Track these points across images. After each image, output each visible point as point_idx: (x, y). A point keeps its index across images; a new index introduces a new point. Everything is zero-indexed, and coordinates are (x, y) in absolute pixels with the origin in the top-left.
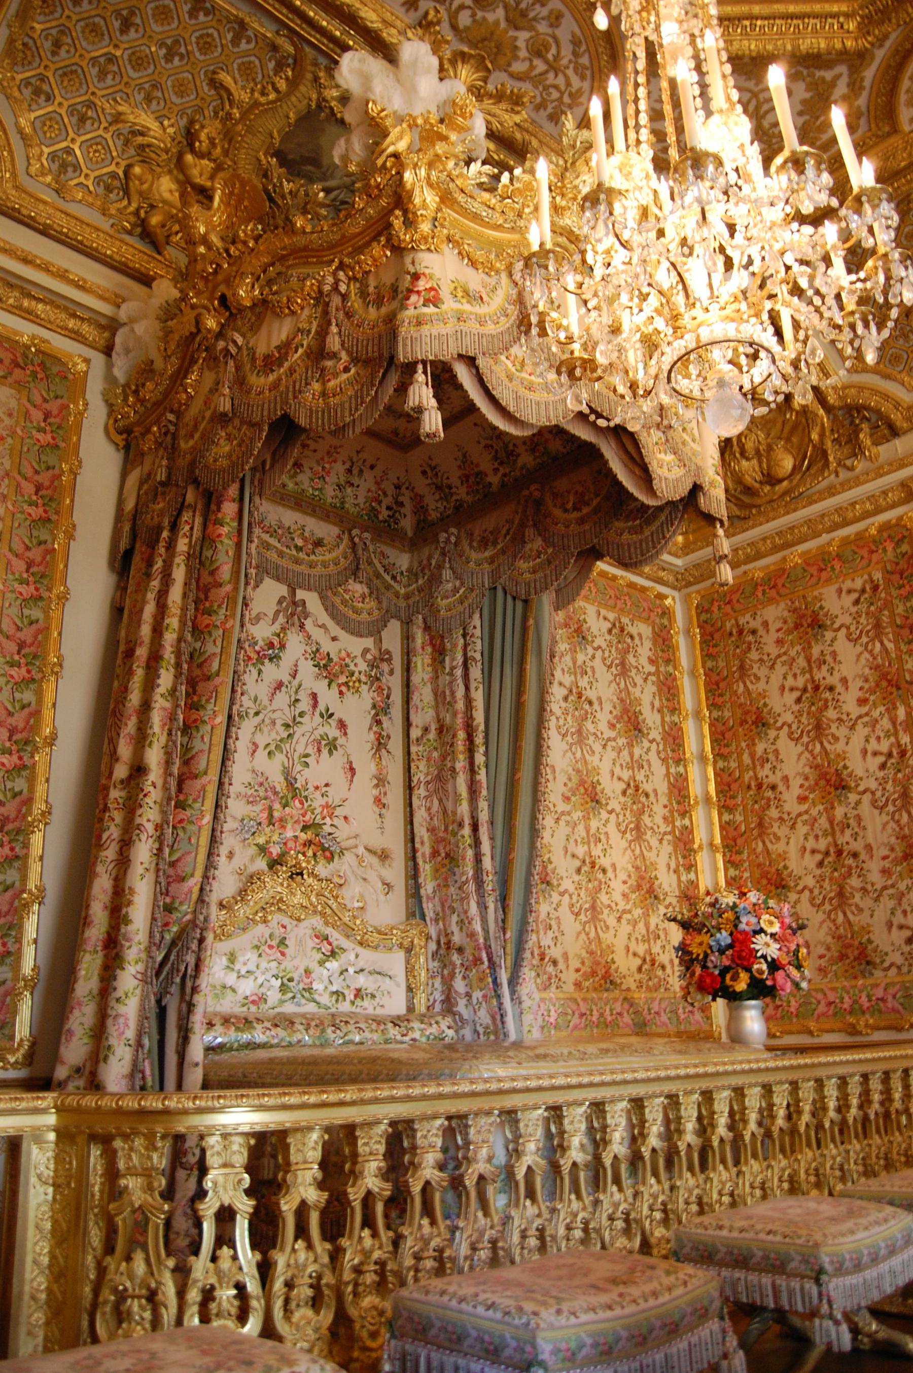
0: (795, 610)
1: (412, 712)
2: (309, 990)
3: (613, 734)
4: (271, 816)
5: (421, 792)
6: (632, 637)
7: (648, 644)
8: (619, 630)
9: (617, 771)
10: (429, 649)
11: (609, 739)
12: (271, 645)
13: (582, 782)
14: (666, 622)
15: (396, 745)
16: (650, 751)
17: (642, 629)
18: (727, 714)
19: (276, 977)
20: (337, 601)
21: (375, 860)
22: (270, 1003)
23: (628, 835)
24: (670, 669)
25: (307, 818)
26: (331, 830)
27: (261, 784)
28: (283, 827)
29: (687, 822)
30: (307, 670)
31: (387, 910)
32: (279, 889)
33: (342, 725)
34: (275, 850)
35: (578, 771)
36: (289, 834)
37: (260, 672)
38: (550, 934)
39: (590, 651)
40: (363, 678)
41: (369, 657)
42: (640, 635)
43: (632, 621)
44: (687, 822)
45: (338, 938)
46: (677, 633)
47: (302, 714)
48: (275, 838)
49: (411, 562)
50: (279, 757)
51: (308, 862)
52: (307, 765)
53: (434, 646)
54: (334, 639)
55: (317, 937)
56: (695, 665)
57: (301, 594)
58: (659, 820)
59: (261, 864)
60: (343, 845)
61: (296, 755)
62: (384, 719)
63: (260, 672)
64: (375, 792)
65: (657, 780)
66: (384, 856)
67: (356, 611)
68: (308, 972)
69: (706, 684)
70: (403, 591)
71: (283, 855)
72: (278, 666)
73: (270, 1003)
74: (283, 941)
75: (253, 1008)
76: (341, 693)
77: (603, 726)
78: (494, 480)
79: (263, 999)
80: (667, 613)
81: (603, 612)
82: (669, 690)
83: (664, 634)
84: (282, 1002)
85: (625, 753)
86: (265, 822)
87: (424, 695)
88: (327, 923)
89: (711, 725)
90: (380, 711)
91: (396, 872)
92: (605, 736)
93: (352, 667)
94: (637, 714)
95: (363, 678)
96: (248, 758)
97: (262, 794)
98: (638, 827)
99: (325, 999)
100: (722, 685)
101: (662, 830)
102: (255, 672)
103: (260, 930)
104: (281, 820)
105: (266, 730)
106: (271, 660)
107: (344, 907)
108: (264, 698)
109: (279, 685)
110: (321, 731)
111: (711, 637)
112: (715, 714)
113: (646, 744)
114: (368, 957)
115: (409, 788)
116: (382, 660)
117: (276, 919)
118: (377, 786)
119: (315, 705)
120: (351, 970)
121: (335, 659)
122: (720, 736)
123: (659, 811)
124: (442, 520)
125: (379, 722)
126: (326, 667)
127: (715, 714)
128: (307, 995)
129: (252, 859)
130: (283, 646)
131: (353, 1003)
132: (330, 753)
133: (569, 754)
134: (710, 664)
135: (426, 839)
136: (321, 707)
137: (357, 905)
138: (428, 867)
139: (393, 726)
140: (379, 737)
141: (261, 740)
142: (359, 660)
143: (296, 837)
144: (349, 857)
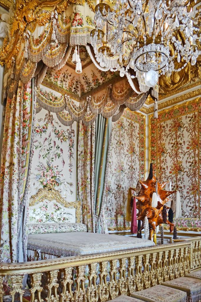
0: (175, 122)
1: (78, 147)
2: (53, 218)
3: (127, 153)
4: (44, 174)
5: (80, 168)
6: (134, 127)
7: (138, 129)
8: (131, 125)
9: (128, 163)
10: (83, 130)
11: (127, 155)
12: (44, 128)
13: (119, 166)
14: (143, 123)
15: (75, 155)
16: (136, 158)
17: (137, 125)
18: (155, 149)
19: (45, 215)
20: (61, 115)
21: (69, 185)
22: (43, 221)
23: (129, 179)
24: (143, 136)
25: (53, 175)
26: (59, 178)
27: (42, 166)
28: (47, 177)
29: (143, 176)
30: (53, 134)
31: (71, 198)
32: (46, 193)
33: (62, 150)
34: (45, 183)
35: (119, 163)
36: (48, 179)
37: (41, 135)
38: (109, 203)
39: (124, 131)
40: (67, 137)
41: (69, 131)
42: (136, 126)
43: (135, 122)
44: (143, 176)
45: (60, 205)
46: (145, 126)
48: (45, 180)
49: (80, 105)
50: (46, 159)
51: (53, 186)
53: (84, 129)
54: (60, 126)
55: (55, 205)
56: (149, 135)
58: (137, 175)
59: (41, 187)
60: (62, 182)
61: (50, 158)
62: (72, 149)
63: (41, 135)
64: (69, 168)
65: (137, 166)
66: (71, 185)
67: (66, 119)
69: (151, 140)
70: (77, 113)
71: (46, 184)
72: (45, 133)
73: (43, 221)
74: (46, 207)
75: (40, 223)
76: (61, 141)
77: (125, 151)
78: (101, 81)
79: (42, 220)
80: (144, 120)
81: (128, 120)
82: (142, 141)
83: (142, 126)
85: (130, 158)
86: (42, 176)
87: (81, 143)
88: (57, 202)
89: (151, 151)
90: (71, 146)
91: (74, 188)
92: (126, 154)
93: (64, 134)
94: (134, 148)
95: (67, 137)
97: (42, 169)
98: (132, 177)
99: (56, 220)
100: (155, 141)
101: (137, 178)
102: (40, 135)
103: (41, 204)
104: (46, 175)
106: (44, 132)
107: (61, 198)
108: (42, 143)
109: (46, 139)
110: (56, 152)
111: (153, 128)
112: (152, 149)
113: (135, 156)
114: (67, 210)
115: (77, 168)
116: (72, 132)
117: (45, 200)
118: (70, 166)
119: (55, 145)
120: (63, 213)
121: (60, 132)
122: (153, 155)
123: (137, 173)
124: (88, 93)
125: (71, 150)
126: (57, 134)
127: (152, 149)
128: (52, 219)
129: (39, 185)
130: (47, 128)
131: (63, 221)
132: (59, 157)
133: (117, 158)
134: (152, 135)
135: (80, 181)
136: (57, 145)
137: (64, 197)
138: (80, 187)
139: (74, 150)
140: (71, 153)
141: (42, 154)
142: (66, 133)
143: (50, 180)
144: (63, 185)
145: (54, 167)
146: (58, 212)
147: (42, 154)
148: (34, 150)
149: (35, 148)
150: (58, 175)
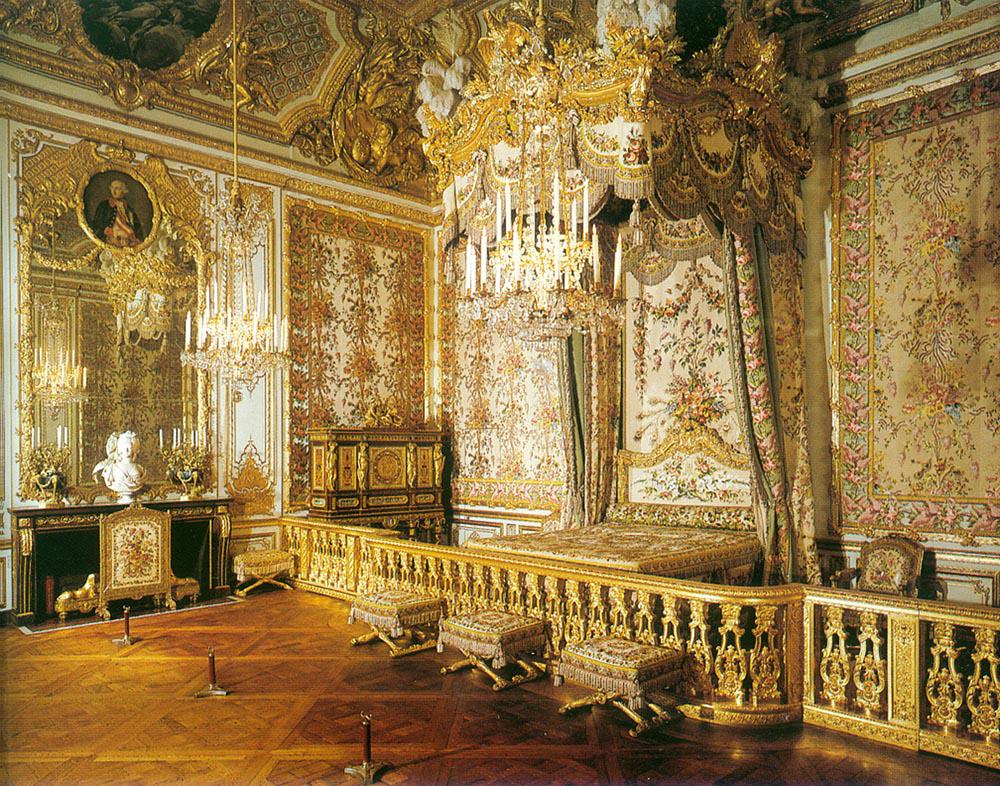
28: (690, 403)
30: (704, 306)
36: (694, 407)
45: (711, 461)
47: (700, 337)
52: (705, 365)
57: (699, 261)
68: (693, 482)
79: (670, 494)
84: (679, 496)
96: (670, 370)
102: (673, 320)
103: (669, 460)
105: (680, 351)
108: (679, 336)
109: (688, 322)
120: (720, 481)
129: (675, 423)
136: (714, 327)
145: (707, 377)
146: (708, 477)
147: (678, 357)
148: (662, 354)
149: (663, 349)
150: (718, 395)
